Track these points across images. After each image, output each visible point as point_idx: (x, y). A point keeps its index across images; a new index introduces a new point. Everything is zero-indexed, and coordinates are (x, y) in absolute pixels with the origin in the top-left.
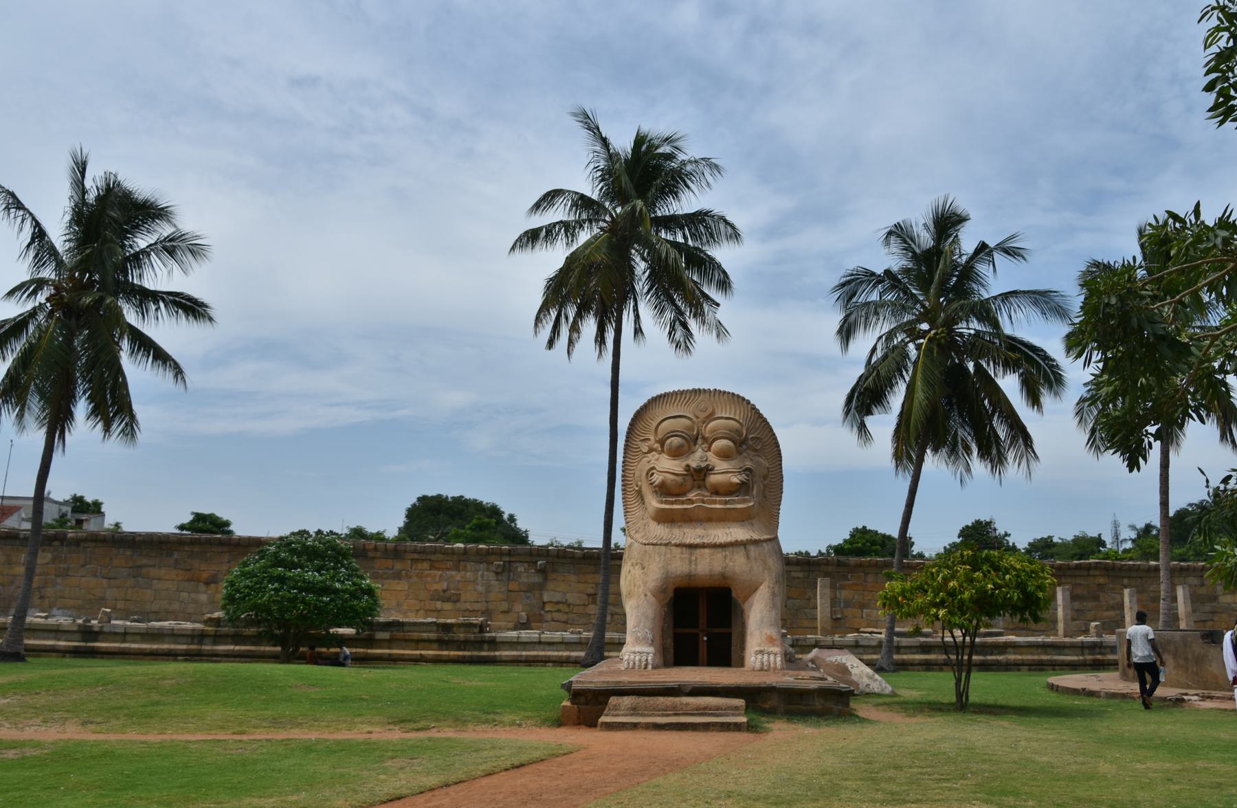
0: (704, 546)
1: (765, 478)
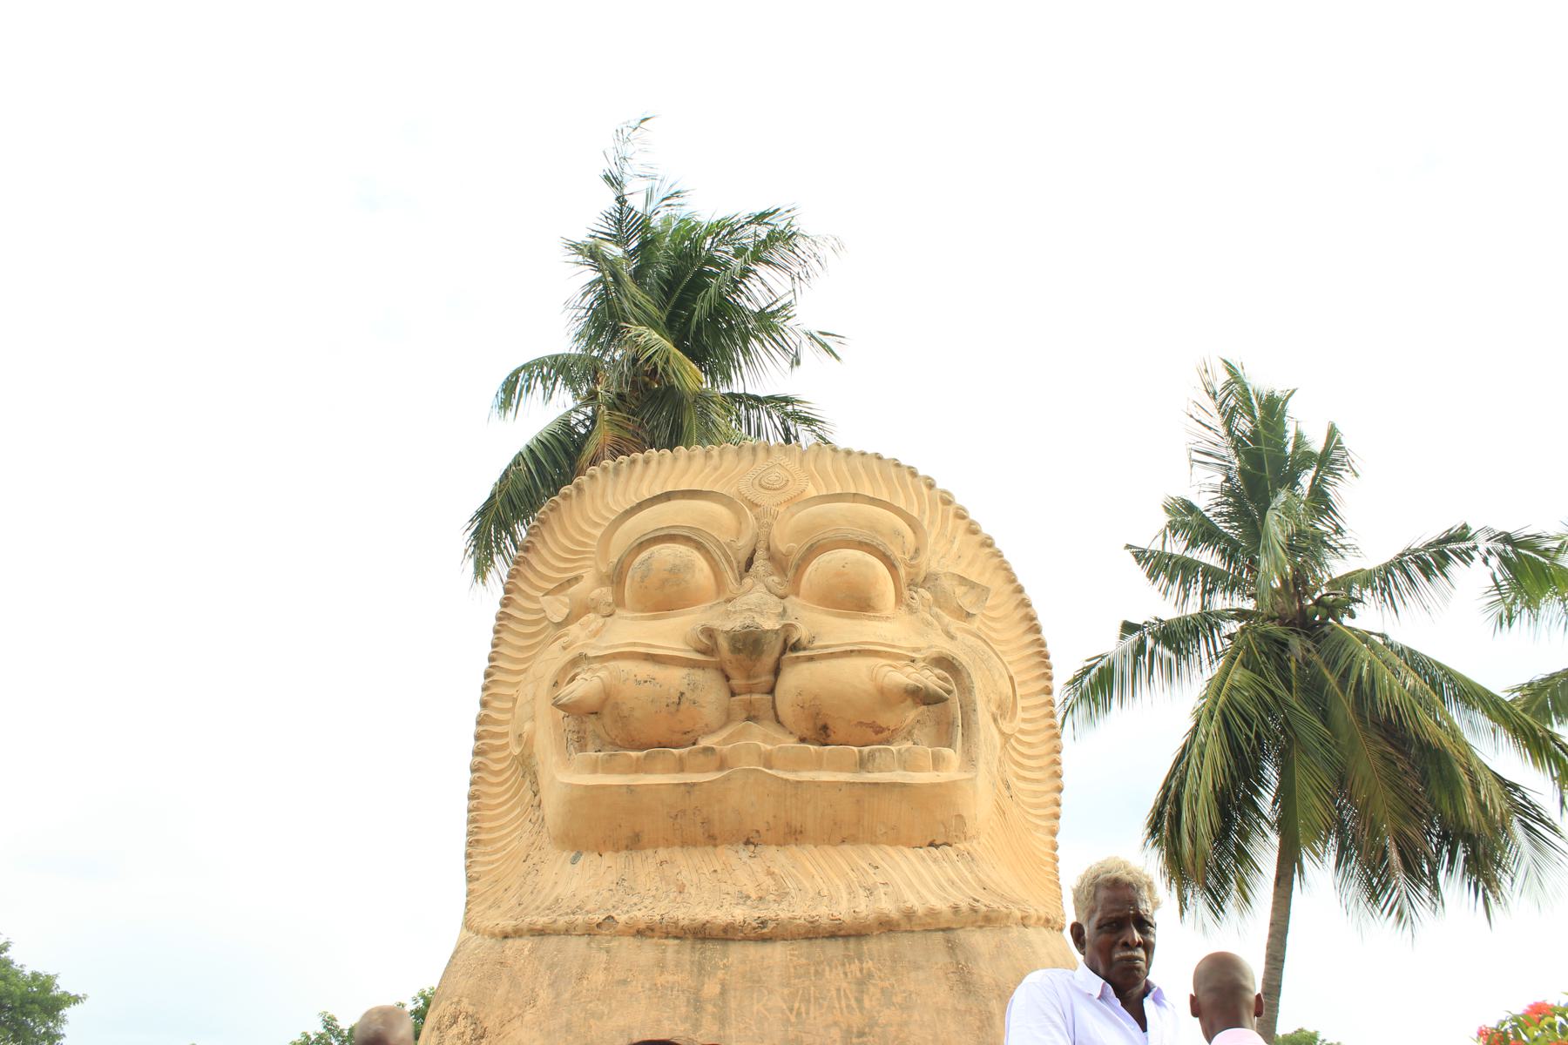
0: (763, 934)
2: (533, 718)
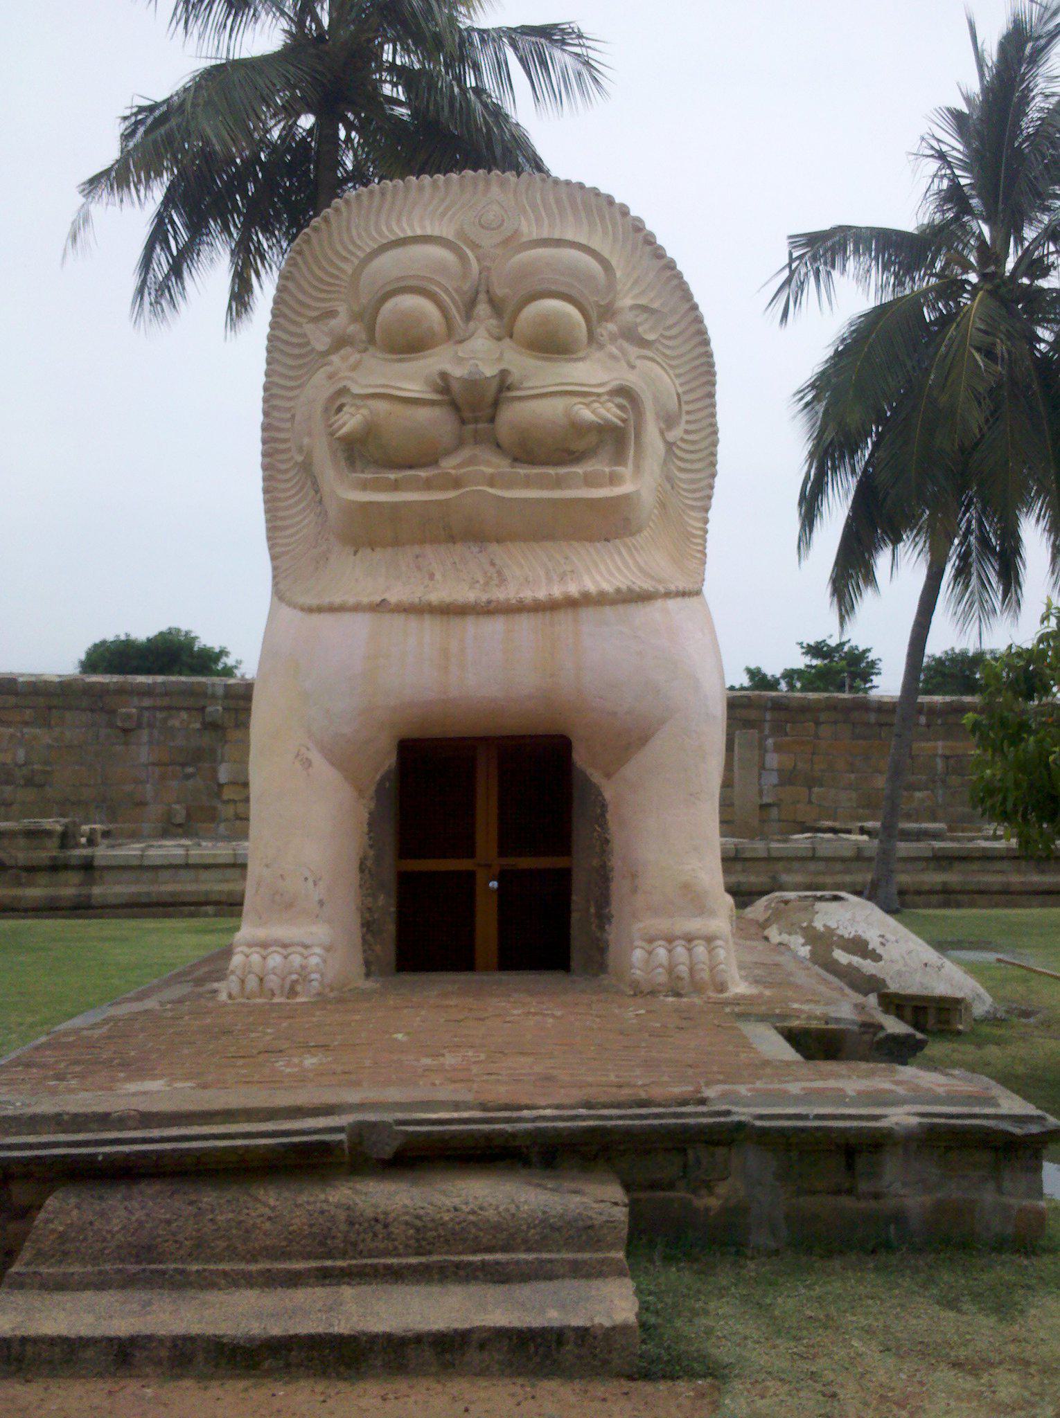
2: (310, 435)
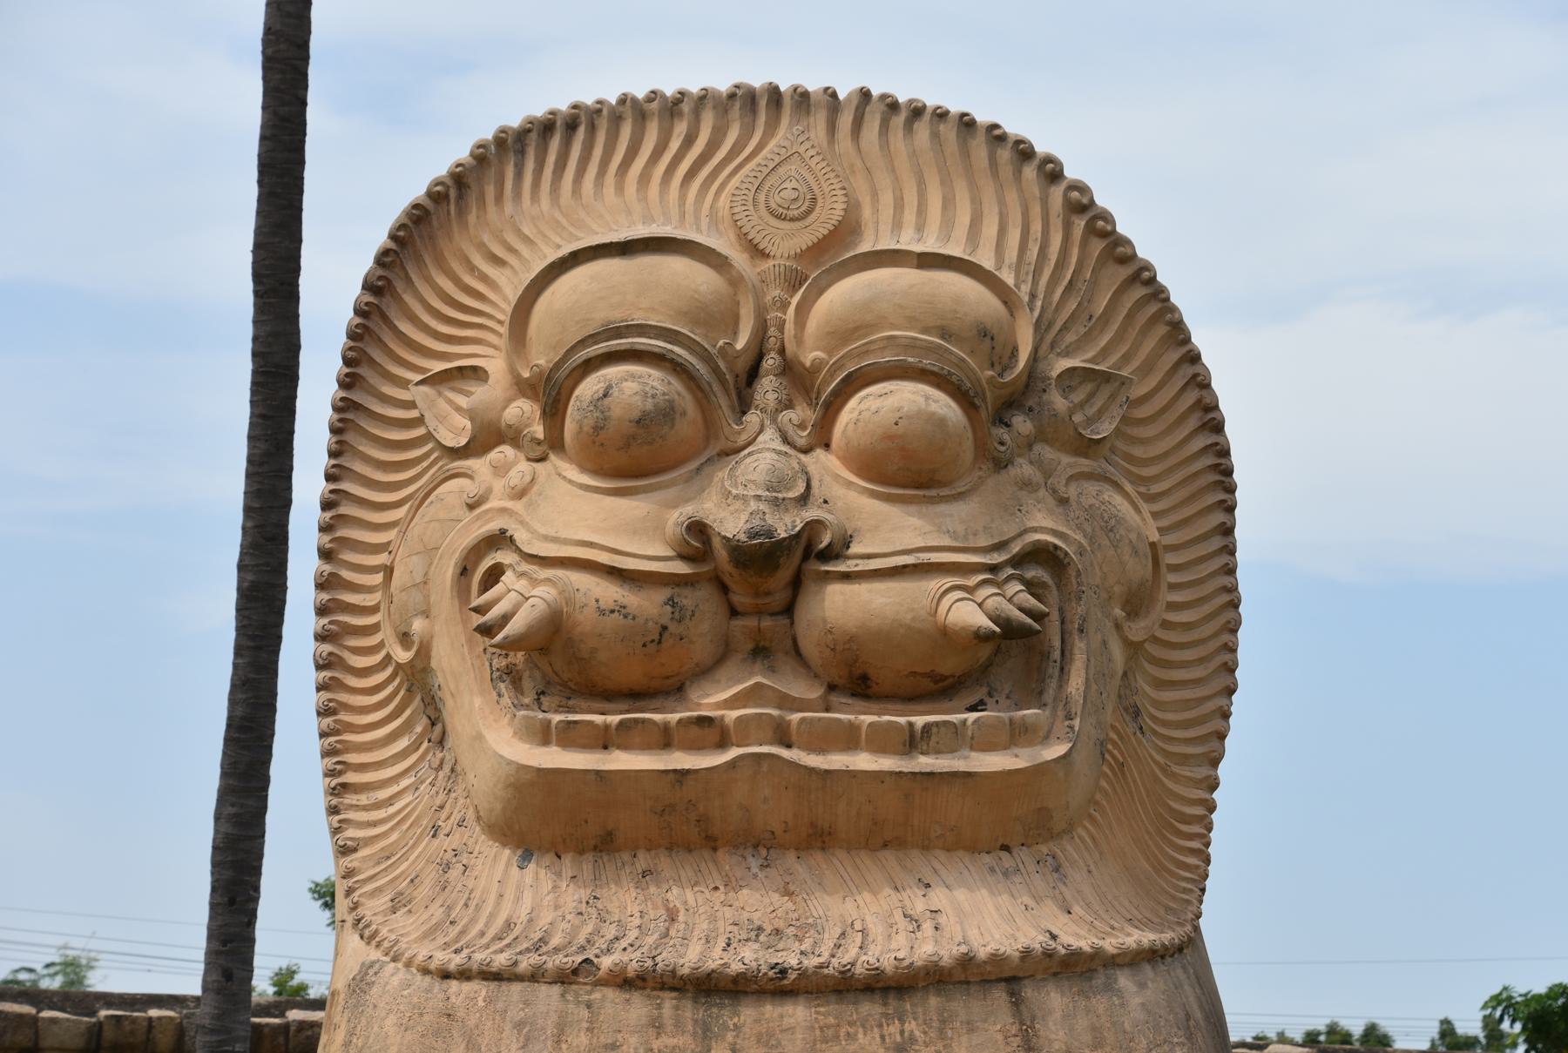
0: (779, 986)
1: (1136, 603)
2: (426, 614)
